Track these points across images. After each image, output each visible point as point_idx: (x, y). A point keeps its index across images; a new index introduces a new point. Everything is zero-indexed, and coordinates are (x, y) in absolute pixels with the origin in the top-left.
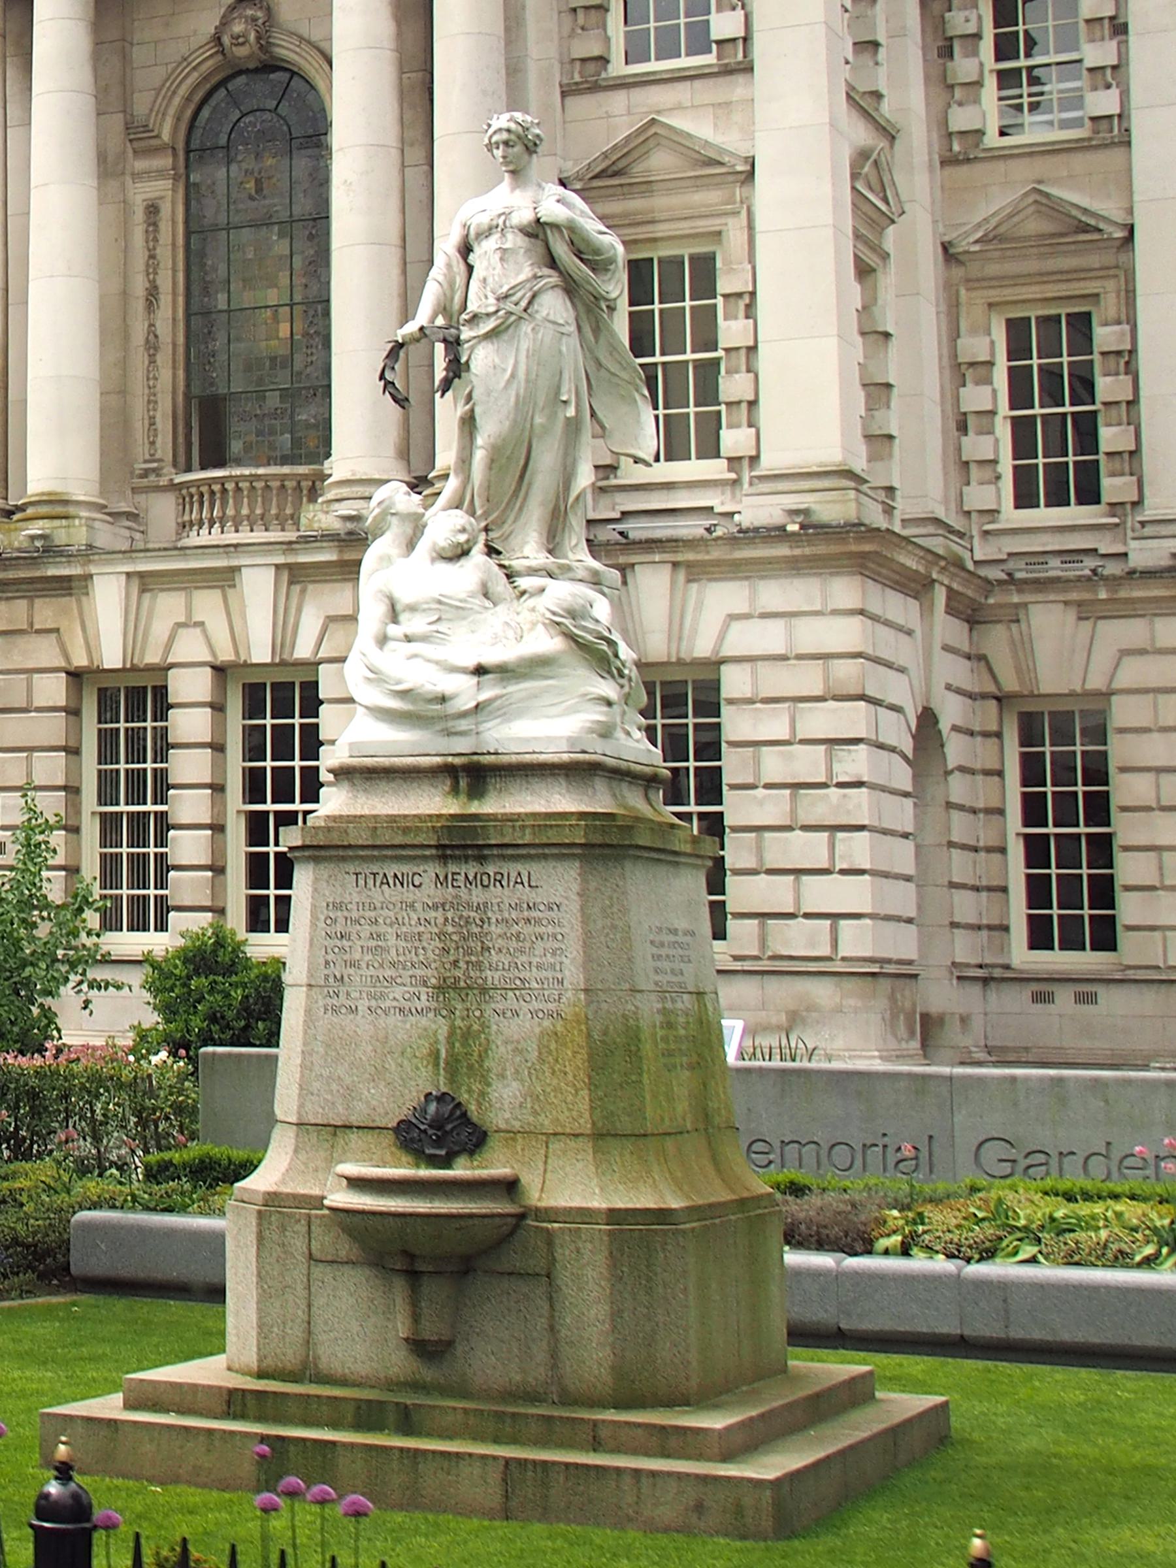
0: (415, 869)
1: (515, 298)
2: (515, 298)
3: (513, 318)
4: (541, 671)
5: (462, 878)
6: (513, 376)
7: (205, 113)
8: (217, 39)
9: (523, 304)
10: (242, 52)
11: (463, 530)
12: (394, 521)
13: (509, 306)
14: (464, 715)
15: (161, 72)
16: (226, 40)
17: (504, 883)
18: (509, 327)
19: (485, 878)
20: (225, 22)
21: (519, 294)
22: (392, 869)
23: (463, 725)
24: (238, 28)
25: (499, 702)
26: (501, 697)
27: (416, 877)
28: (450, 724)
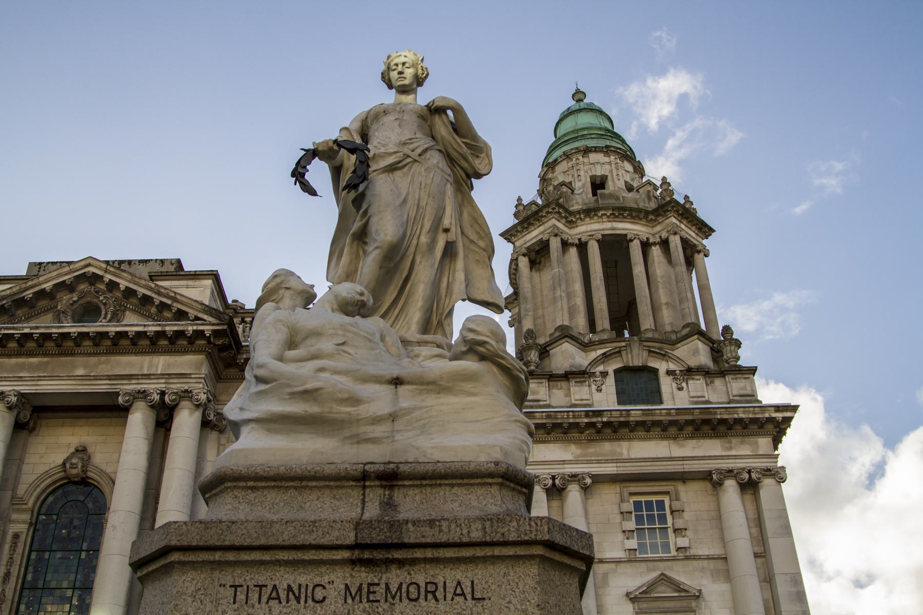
0: (317, 580)
1: (411, 146)
2: (411, 146)
3: (409, 160)
4: (468, 386)
5: (381, 590)
6: (405, 201)
7: (51, 499)
8: (64, 464)
9: (419, 151)
10: (74, 471)
11: (362, 294)
12: (288, 294)
13: (406, 150)
14: (376, 420)
15: (34, 477)
16: (68, 465)
17: (440, 594)
18: (405, 166)
19: (412, 589)
20: (68, 458)
21: (416, 145)
22: (285, 578)
23: (378, 431)
24: (74, 461)
25: (417, 413)
26: (421, 408)
27: (318, 589)
28: (363, 429)
